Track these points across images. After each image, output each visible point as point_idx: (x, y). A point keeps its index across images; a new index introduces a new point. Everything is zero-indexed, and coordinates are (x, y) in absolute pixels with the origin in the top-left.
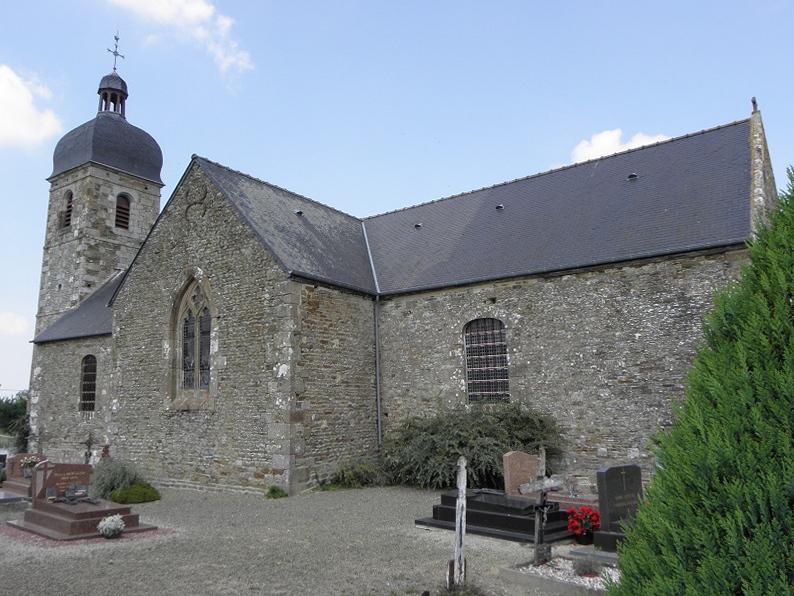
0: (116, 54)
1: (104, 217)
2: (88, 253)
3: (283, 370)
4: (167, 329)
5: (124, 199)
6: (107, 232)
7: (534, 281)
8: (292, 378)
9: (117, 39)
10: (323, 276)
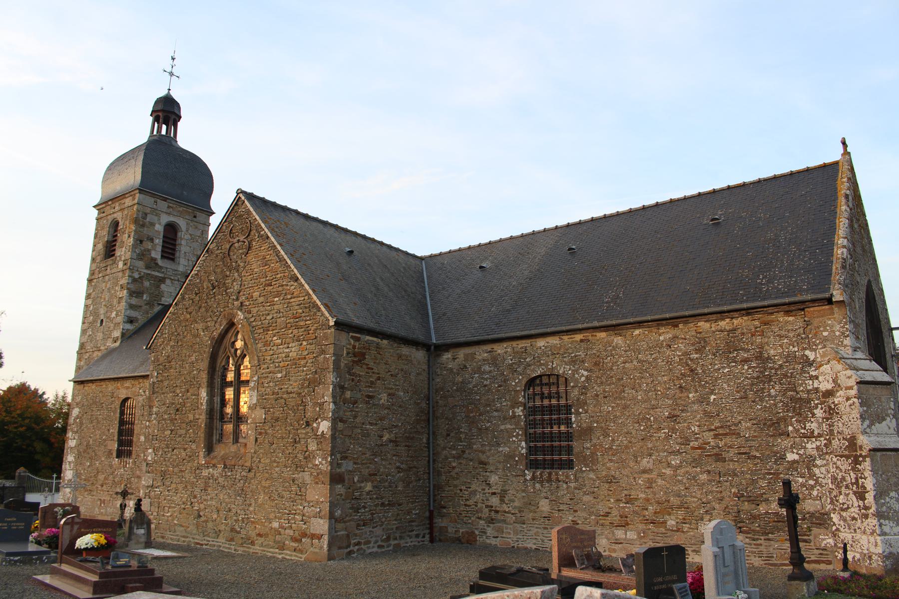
0: (171, 74)
1: (150, 247)
2: (131, 286)
3: (324, 426)
4: (204, 376)
5: (171, 230)
7: (602, 335)
8: (333, 437)
9: (173, 59)
10: (371, 324)
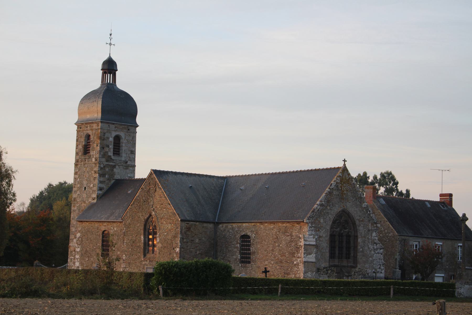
0: (110, 44)
1: (107, 150)
2: (100, 172)
3: (178, 250)
4: (142, 231)
5: (117, 139)
6: (109, 159)
7: (258, 224)
8: (180, 253)
9: (111, 35)
10: (193, 219)
